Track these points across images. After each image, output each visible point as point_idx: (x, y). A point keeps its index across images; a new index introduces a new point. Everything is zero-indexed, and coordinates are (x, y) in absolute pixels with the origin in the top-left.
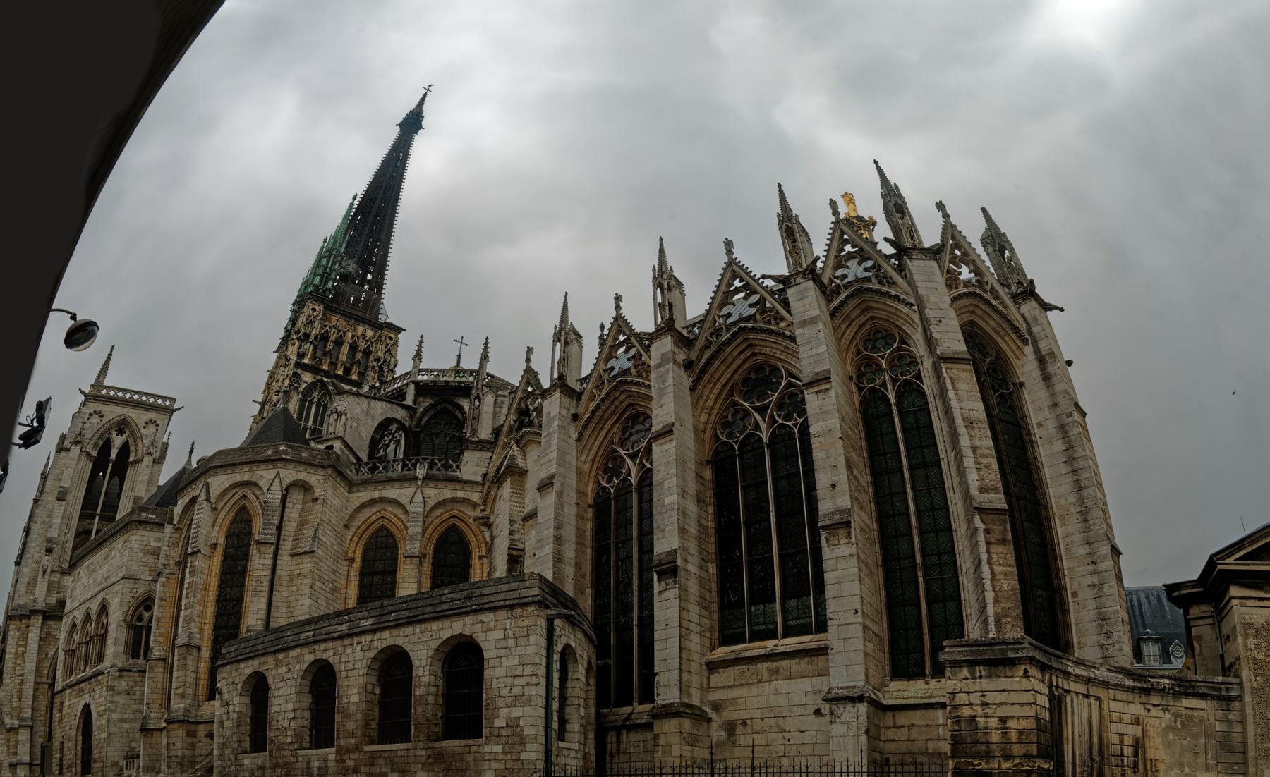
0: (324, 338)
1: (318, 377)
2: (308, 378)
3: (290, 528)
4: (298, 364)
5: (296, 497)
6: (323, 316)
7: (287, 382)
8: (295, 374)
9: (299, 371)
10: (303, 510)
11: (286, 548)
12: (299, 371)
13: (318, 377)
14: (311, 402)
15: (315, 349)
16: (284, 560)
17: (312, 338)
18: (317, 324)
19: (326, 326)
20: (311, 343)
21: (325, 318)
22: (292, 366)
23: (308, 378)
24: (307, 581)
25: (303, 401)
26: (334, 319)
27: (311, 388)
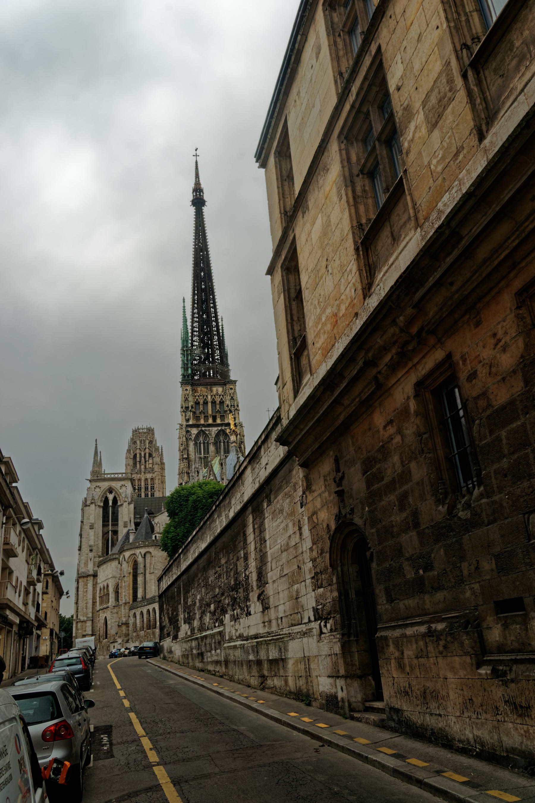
0: (197, 403)
1: (200, 429)
2: (194, 431)
3: (148, 565)
4: (187, 426)
5: (148, 556)
6: (192, 391)
7: (184, 438)
8: (187, 432)
9: (189, 429)
10: (151, 559)
11: (148, 572)
12: (189, 429)
13: (200, 429)
14: (200, 443)
15: (194, 413)
16: (148, 575)
17: (190, 408)
18: (191, 399)
19: (196, 396)
20: (190, 411)
21: (194, 391)
22: (184, 429)
23: (194, 431)
24: (153, 581)
25: (195, 444)
26: (199, 389)
27: (198, 435)
